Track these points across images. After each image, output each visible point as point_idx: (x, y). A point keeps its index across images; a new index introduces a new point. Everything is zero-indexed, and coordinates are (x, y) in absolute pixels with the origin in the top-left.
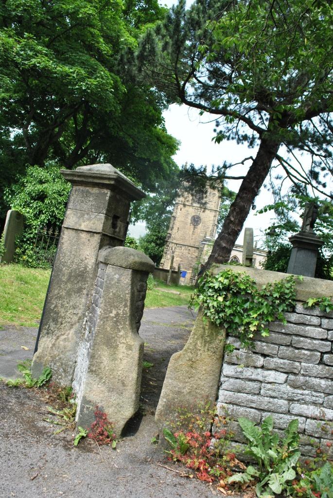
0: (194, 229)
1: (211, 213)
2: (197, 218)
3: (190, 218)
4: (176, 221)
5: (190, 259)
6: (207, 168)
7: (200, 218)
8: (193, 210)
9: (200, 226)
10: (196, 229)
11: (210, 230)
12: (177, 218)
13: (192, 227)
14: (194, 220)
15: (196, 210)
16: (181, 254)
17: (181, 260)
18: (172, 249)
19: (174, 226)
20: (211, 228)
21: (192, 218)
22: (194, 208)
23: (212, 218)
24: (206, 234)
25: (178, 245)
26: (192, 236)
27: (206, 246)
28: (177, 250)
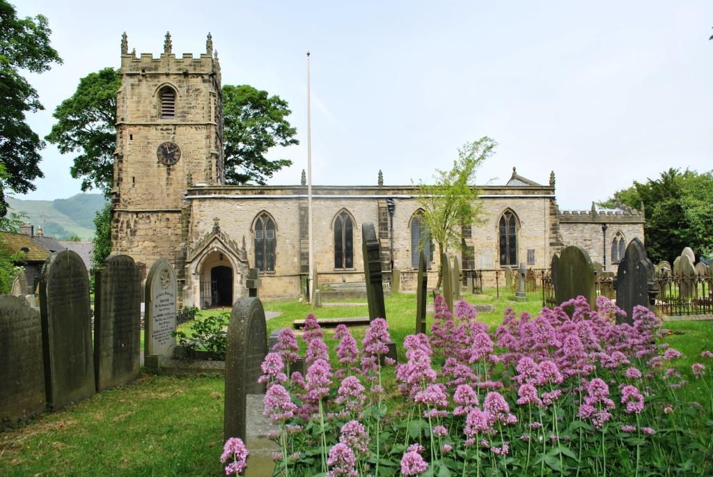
0: (169, 174)
1: (199, 132)
2: (170, 149)
3: (154, 151)
4: (125, 165)
5: (173, 238)
6: (171, 39)
7: (175, 147)
8: (159, 133)
9: (180, 165)
10: (172, 173)
11: (203, 169)
12: (125, 158)
13: (163, 169)
14: (165, 154)
15: (165, 132)
16: (151, 232)
17: (154, 244)
18: (128, 226)
19: (123, 175)
20: (204, 163)
21: (159, 150)
22: (159, 127)
23: (204, 142)
24: (190, 176)
25: (140, 216)
26: (168, 189)
27: (195, 203)
28: (139, 226)
